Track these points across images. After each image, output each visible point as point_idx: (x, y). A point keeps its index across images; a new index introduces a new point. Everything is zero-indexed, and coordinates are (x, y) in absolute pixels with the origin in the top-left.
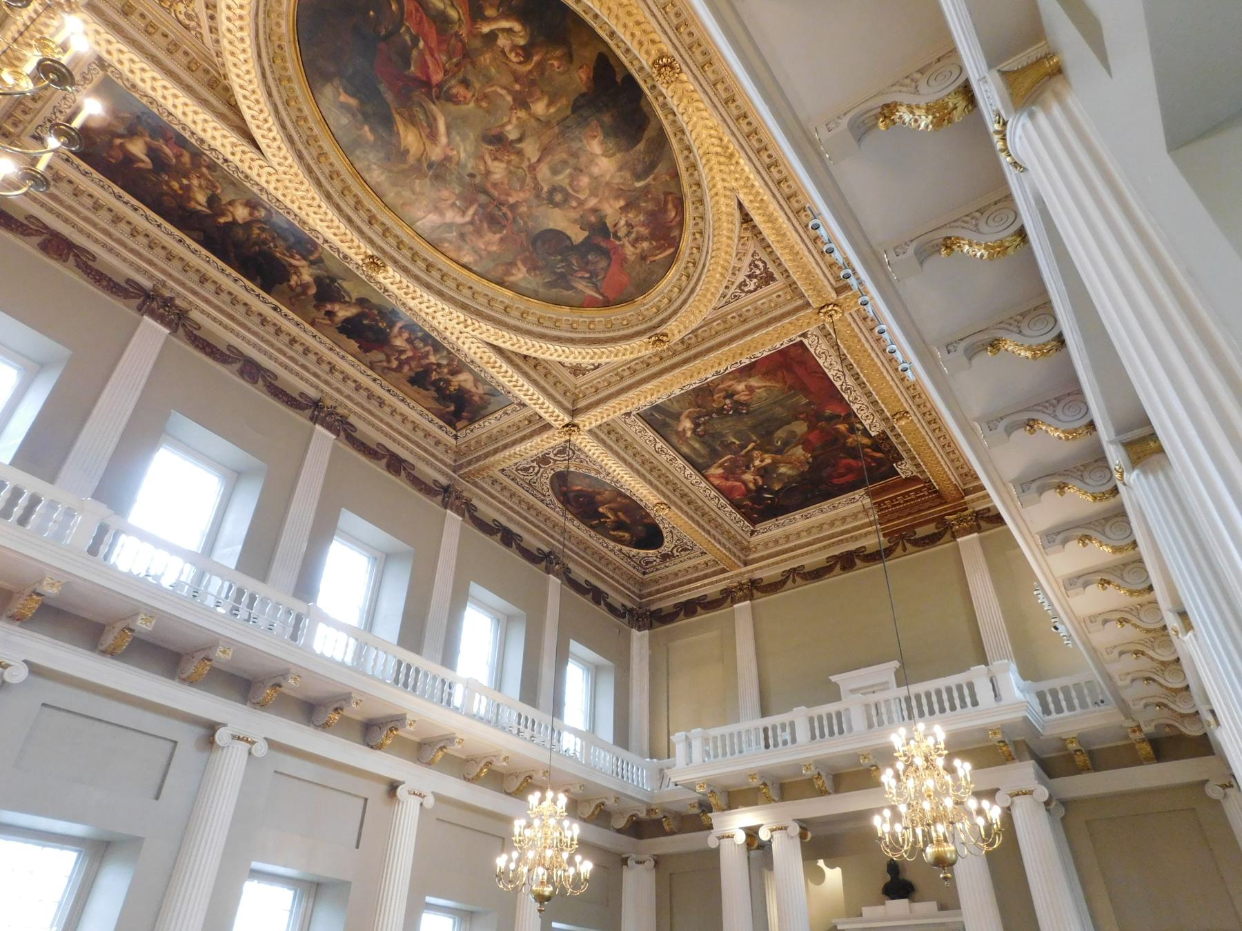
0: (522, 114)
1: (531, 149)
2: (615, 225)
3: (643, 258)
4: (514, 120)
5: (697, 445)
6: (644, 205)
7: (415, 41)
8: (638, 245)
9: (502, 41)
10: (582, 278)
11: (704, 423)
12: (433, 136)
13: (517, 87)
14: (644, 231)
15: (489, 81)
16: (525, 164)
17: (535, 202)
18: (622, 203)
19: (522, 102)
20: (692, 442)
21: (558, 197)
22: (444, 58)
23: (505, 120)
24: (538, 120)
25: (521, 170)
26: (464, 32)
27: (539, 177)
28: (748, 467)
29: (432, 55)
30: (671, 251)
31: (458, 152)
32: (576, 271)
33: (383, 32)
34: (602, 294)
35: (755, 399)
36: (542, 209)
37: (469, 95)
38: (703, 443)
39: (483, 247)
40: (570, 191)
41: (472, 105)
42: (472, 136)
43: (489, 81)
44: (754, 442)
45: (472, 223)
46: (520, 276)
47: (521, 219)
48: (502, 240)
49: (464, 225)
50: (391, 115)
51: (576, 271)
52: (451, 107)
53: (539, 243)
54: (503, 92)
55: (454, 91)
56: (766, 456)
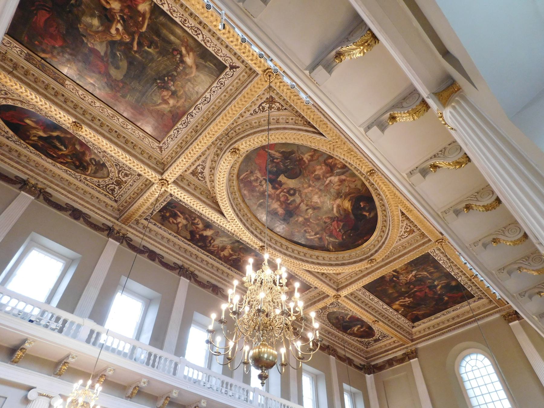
0: (307, 217)
1: (303, 207)
3: (252, 172)
4: (309, 215)
5: (172, 38)
7: (340, 231)
8: (255, 177)
9: (313, 234)
10: (277, 159)
11: (178, 64)
12: (339, 206)
13: (308, 224)
14: (255, 184)
15: (317, 224)
16: (305, 202)
17: (301, 189)
19: (307, 220)
20: (177, 41)
21: (292, 192)
23: (312, 215)
24: (302, 216)
26: (325, 234)
27: (300, 198)
28: (122, 17)
29: (335, 229)
30: (241, 177)
31: (330, 202)
32: (281, 162)
33: (349, 231)
34: (267, 152)
35: (158, 94)
36: (299, 187)
37: (324, 220)
38: (170, 42)
40: (287, 195)
41: (324, 217)
42: (325, 209)
43: (317, 224)
44: (136, 52)
45: (327, 177)
46: (306, 156)
47: (306, 182)
48: (315, 171)
49: (331, 176)
51: (280, 162)
52: (330, 215)
54: (313, 222)
55: (329, 220)
56: (118, 38)
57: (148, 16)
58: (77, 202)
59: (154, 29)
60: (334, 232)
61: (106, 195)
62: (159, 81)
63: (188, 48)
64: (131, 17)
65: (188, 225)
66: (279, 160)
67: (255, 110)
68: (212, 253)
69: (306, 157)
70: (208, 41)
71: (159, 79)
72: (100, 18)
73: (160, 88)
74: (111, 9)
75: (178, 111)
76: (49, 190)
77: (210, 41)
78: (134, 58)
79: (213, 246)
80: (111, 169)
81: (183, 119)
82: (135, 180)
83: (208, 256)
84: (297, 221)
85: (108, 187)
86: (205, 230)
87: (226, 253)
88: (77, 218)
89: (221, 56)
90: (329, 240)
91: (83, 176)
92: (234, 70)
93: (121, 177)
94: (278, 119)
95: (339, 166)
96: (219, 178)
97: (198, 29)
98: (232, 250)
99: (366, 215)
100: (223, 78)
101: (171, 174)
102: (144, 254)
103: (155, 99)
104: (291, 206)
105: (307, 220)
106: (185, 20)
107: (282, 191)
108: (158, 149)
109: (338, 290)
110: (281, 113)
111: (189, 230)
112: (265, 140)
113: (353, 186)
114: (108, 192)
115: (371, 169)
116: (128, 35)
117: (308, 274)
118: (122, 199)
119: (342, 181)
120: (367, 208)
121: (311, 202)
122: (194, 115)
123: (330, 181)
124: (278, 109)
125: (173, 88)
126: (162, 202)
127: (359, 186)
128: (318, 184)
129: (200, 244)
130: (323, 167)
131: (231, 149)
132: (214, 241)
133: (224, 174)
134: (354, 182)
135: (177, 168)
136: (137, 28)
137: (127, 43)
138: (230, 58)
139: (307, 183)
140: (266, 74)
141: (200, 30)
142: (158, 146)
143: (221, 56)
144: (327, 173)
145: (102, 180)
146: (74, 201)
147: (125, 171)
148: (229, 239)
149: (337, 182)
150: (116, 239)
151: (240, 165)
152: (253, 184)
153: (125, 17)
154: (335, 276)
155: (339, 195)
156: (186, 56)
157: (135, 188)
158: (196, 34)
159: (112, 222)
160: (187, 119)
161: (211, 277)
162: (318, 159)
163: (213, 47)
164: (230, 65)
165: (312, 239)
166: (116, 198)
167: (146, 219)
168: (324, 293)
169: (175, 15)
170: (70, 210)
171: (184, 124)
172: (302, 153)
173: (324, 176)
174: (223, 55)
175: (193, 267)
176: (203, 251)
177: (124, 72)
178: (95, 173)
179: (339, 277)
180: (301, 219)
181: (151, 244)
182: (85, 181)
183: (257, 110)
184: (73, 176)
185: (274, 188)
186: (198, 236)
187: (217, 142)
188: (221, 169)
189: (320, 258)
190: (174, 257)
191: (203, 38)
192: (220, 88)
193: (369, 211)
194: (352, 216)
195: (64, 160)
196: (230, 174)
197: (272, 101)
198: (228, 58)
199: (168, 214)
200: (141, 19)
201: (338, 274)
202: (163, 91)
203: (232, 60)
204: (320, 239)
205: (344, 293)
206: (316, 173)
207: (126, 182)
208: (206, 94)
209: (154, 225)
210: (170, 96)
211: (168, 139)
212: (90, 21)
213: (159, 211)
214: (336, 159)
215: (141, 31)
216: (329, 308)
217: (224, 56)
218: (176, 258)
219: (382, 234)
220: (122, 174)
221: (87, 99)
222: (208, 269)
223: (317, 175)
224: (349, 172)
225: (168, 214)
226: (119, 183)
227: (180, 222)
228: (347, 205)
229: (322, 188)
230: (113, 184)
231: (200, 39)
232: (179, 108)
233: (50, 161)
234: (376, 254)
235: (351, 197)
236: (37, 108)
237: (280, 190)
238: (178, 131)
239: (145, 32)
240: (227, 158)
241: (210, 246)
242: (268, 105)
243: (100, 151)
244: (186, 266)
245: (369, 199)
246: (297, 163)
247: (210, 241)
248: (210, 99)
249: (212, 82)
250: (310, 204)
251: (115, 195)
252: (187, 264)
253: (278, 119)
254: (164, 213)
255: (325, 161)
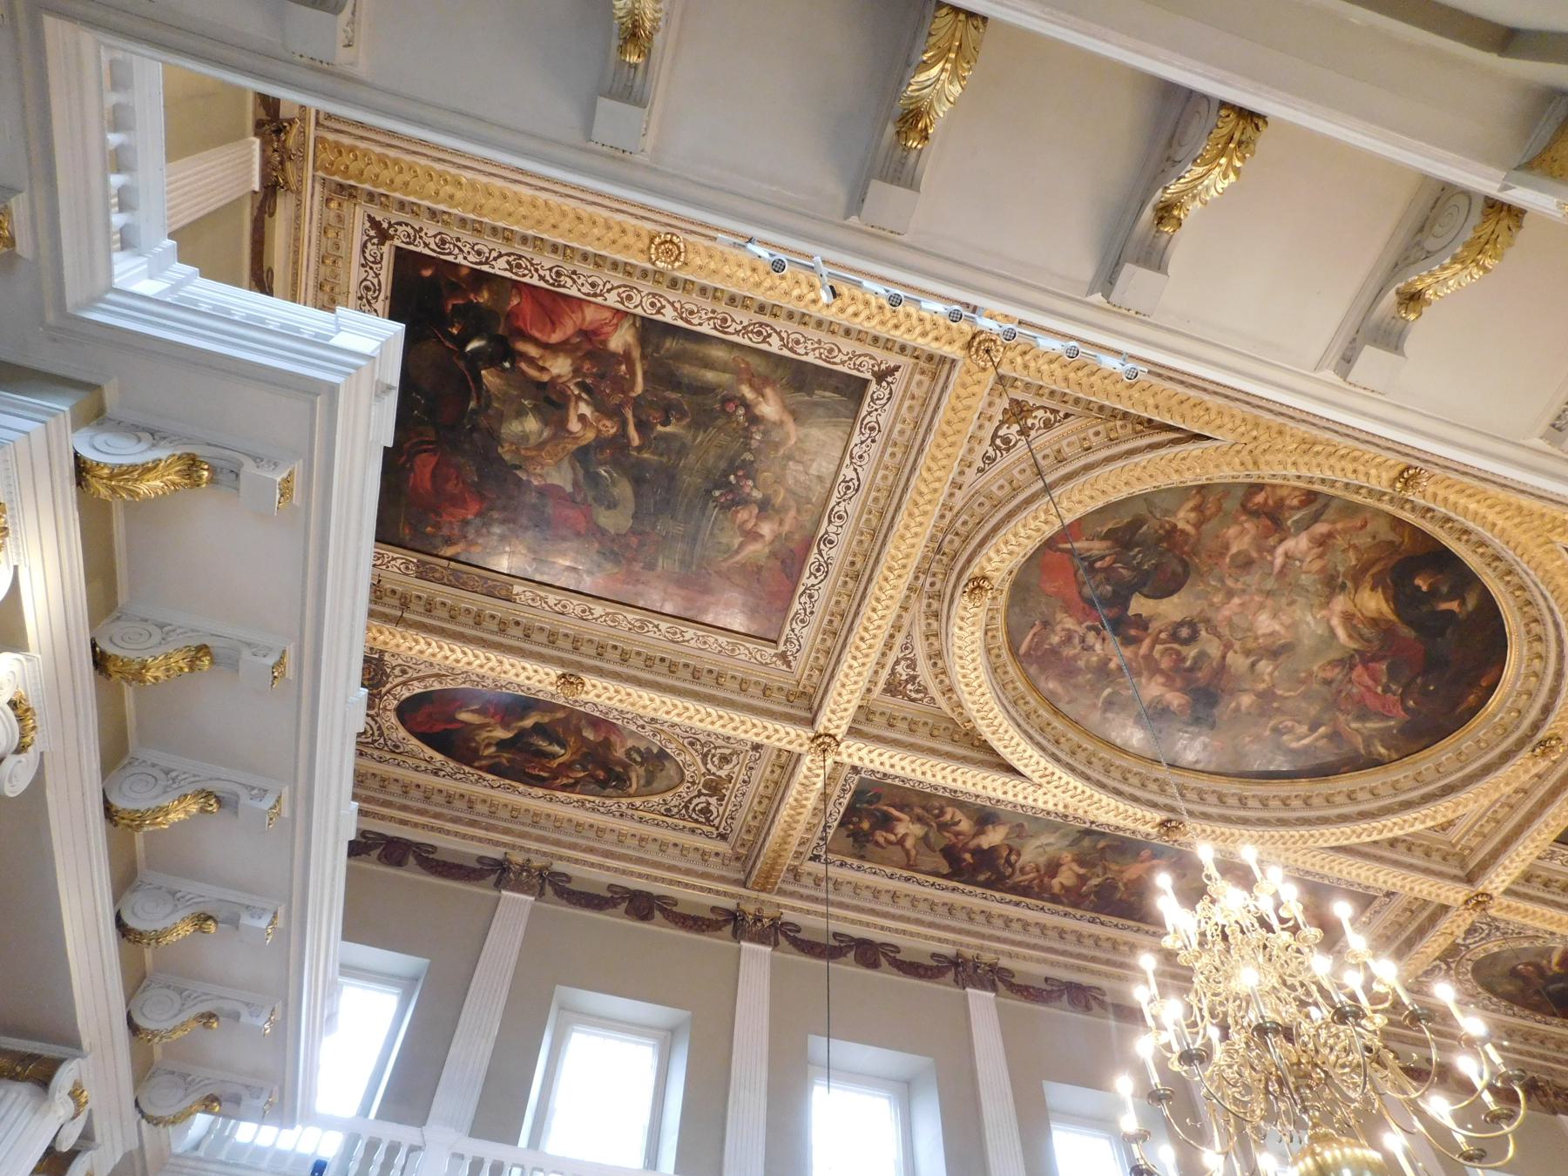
0: (1262, 686)
1: (1237, 661)
2: (1104, 639)
3: (1046, 624)
4: (1267, 678)
5: (710, 376)
6: (1089, 676)
7: (1386, 689)
8: (1063, 633)
9: (1304, 729)
10: (1102, 558)
11: (746, 429)
12: (1348, 618)
13: (1275, 705)
14: (1068, 652)
15: (1305, 696)
16: (1237, 645)
17: (1209, 613)
18: (1112, 665)
19: (1266, 696)
20: (726, 378)
21: (1184, 632)
22: (1355, 690)
23: (1276, 673)
25: (1240, 636)
26: (1342, 718)
27: (1216, 641)
28: (583, 386)
29: (1368, 688)
30: (1023, 649)
31: (1314, 618)
33: (1419, 680)
35: (727, 524)
36: (1199, 609)
37: (1321, 675)
38: (707, 390)
39: (1246, 525)
40: (1176, 646)
42: (1306, 642)
44: (639, 449)
45: (1272, 550)
46: (1181, 514)
48: (1227, 547)
49: (1281, 541)
50: (1399, 616)
52: (1335, 655)
53: (1180, 570)
54: (1287, 694)
55: (1337, 670)
56: (590, 435)
57: (636, 354)
58: (632, 874)
59: (661, 376)
60: (1370, 701)
61: (693, 831)
62: (717, 493)
63: (756, 381)
64: (601, 376)
65: (931, 835)
66: (1107, 559)
67: (985, 457)
68: (1025, 891)
69: (1184, 518)
70: (798, 342)
71: (717, 487)
72: (536, 410)
73: (725, 508)
74: (553, 380)
75: (792, 546)
76: (559, 866)
77: (802, 340)
78: (640, 464)
79: (1022, 870)
80: (682, 757)
81: (812, 560)
82: (751, 765)
83: (1017, 904)
84: (1237, 709)
85: (691, 807)
86: (980, 832)
87: (1065, 877)
88: (645, 916)
89: (843, 363)
90: (1365, 731)
91: (625, 801)
92: (889, 379)
93: (713, 769)
94: (1059, 451)
95: (1295, 502)
96: (964, 677)
97: (761, 324)
98: (1081, 863)
99: (1451, 612)
100: (869, 413)
101: (837, 713)
102: (845, 955)
103: (724, 540)
104: (1200, 675)
105: (1266, 696)
106: (724, 320)
107: (1156, 641)
108: (779, 663)
109: (1470, 879)
110: (1058, 431)
111: (938, 849)
112: (1046, 522)
113: (1363, 540)
114: (696, 821)
115: (1400, 467)
116: (610, 417)
117: (1342, 857)
118: (737, 825)
119: (1323, 542)
120: (1445, 589)
121: (1256, 638)
122: (833, 537)
123: (1287, 555)
124: (1048, 425)
125: (757, 495)
126: (839, 797)
127: (1386, 534)
128: (1253, 579)
129: (982, 878)
130: (1246, 525)
131: (967, 585)
132: (1019, 855)
133: (973, 660)
134: (1364, 526)
135: (844, 692)
136: (623, 392)
137: (615, 436)
138: (865, 355)
139: (1219, 590)
140: (977, 351)
141: (767, 325)
142: (776, 655)
143: (843, 363)
144: (1267, 537)
145: (671, 794)
146: (624, 872)
147: (718, 751)
148: (1058, 834)
149: (1310, 549)
150: (761, 939)
151: (1007, 617)
152: (1065, 654)
153: (588, 381)
154: (1440, 836)
155: (1332, 584)
156: (758, 403)
157: (757, 786)
158: (761, 339)
159: (732, 896)
160: (821, 555)
161: (1053, 964)
162: (1220, 509)
163: (814, 350)
164: (874, 374)
165: (1307, 747)
166: (721, 829)
167: (815, 858)
168: (1426, 903)
169: (696, 321)
170: (623, 899)
171: (818, 570)
172: (1167, 512)
173: (1260, 550)
174: (846, 358)
175: (990, 951)
176: (998, 895)
177: (630, 505)
178: (649, 783)
179: (1454, 835)
180: (1246, 700)
181: (853, 922)
182: (634, 812)
183: (991, 453)
184: (602, 809)
185: (1128, 641)
186: (967, 856)
187: (921, 581)
188: (960, 648)
189: (1361, 796)
190: (926, 937)
191: (782, 339)
192: (873, 441)
193: (1457, 593)
194: (1406, 632)
195: (568, 777)
196: (988, 651)
197: (1022, 411)
198: (862, 359)
199: (866, 825)
200: (623, 367)
201: (1444, 828)
202: (738, 512)
203: (872, 358)
204: (1335, 736)
205: (1497, 881)
206: (1234, 550)
207: (730, 779)
208: (844, 471)
209: (841, 865)
210: (758, 517)
211: (794, 625)
212: (520, 428)
213: (841, 824)
214: (1274, 486)
215: (633, 395)
216: (1467, 947)
217: (850, 359)
218: (933, 938)
219: (1538, 647)
220: (713, 762)
221: (570, 609)
222: (1033, 941)
223: (1239, 553)
224: (1334, 504)
225: (866, 825)
226: (714, 787)
227: (905, 835)
228: (1373, 603)
229: (1270, 584)
230: (700, 794)
231: (774, 346)
232: (789, 536)
233: (540, 792)
234: (1552, 718)
235: (1373, 576)
236: (474, 678)
237: (1147, 643)
238: (811, 596)
239: (645, 391)
240: (963, 613)
241: (1013, 872)
242: (1016, 427)
243: (641, 722)
244: (969, 953)
245: (1440, 559)
246: (1165, 545)
247: (1008, 861)
248: (859, 480)
249: (846, 437)
250: (1254, 645)
251: (716, 822)
252: (970, 946)
253: (1059, 451)
254: (854, 824)
255: (1243, 506)
